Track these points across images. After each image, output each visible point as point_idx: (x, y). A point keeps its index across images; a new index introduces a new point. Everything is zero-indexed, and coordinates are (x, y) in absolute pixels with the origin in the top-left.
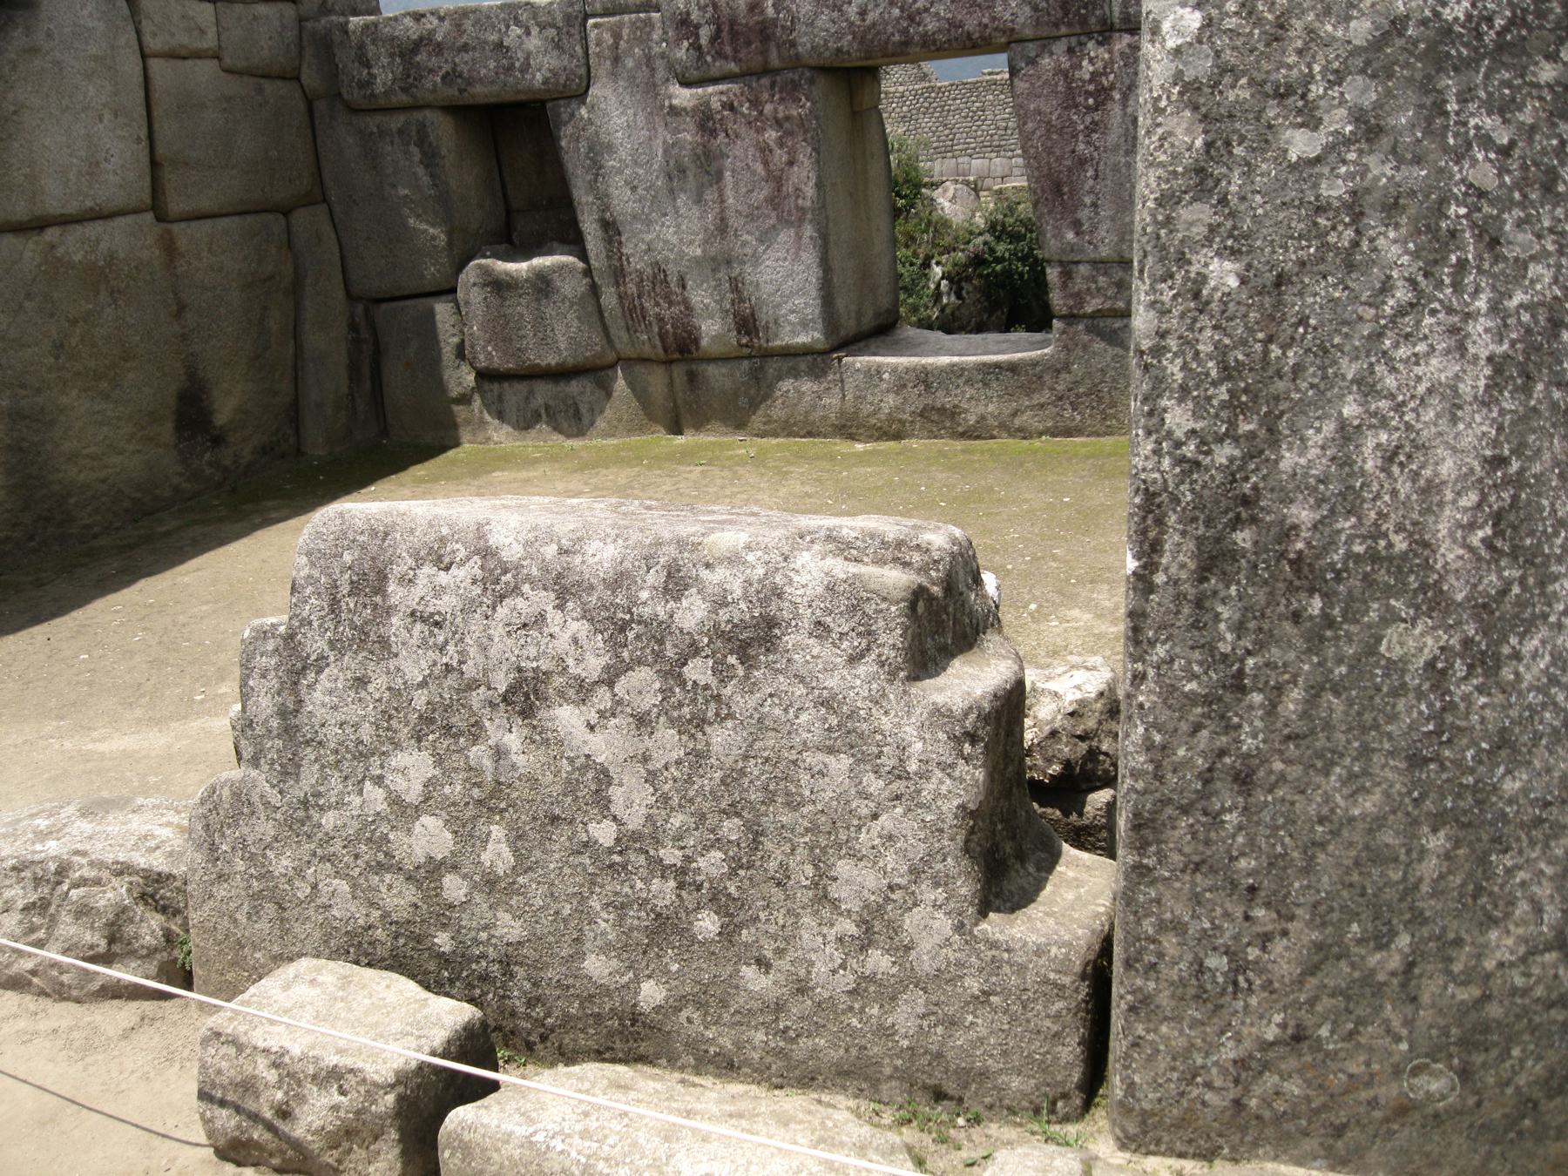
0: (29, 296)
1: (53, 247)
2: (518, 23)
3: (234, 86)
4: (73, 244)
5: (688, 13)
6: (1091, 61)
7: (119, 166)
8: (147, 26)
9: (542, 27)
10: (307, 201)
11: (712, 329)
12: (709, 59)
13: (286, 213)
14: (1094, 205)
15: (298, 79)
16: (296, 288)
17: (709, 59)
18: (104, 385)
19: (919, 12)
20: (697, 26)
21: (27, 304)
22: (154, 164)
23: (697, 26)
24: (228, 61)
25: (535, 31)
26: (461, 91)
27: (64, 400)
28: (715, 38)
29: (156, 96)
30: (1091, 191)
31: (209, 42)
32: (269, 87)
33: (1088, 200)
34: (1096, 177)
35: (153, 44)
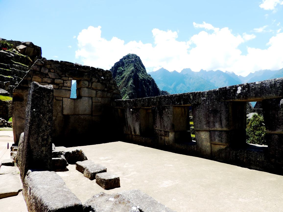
35: (93, 101)
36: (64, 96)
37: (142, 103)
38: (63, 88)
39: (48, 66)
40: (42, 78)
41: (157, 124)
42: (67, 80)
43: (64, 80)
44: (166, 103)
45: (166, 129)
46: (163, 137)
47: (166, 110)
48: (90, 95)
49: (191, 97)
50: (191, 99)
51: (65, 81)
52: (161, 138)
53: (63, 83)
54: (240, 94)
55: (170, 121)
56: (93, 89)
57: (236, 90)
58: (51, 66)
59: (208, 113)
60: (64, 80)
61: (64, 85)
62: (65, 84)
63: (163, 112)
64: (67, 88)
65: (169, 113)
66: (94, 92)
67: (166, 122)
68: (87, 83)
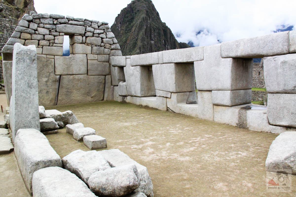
0: (71, 81)
1: (74, 77)
3: (99, 63)
4: (76, 77)
7: (83, 69)
8: (88, 57)
10: (108, 75)
13: (105, 76)
15: (109, 62)
16: (105, 83)
18: (78, 90)
21: (70, 82)
22: (87, 70)
24: (98, 61)
27: (73, 91)
29: (88, 64)
31: (96, 58)
32: (104, 63)
35: (88, 59)
36: (56, 54)
38: (54, 45)
39: (38, 21)
40: (31, 35)
42: (58, 36)
43: (55, 36)
48: (85, 52)
51: (56, 37)
53: (54, 39)
56: (88, 45)
58: (40, 20)
60: (55, 36)
61: (56, 42)
62: (56, 41)
64: (59, 45)
66: (89, 48)
68: (80, 37)
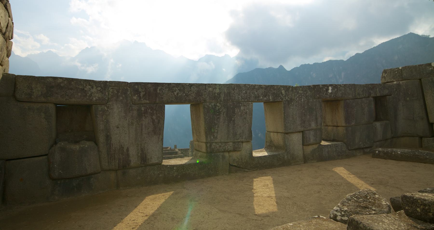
2: (90, 85)
5: (138, 89)
6: (218, 107)
9: (97, 87)
11: (134, 160)
12: (142, 99)
14: (217, 132)
17: (142, 99)
19: (189, 95)
20: (140, 92)
23: (140, 92)
25: (95, 87)
26: (66, 100)
28: (144, 95)
30: (217, 129)
33: (216, 131)
34: (218, 127)
37: (178, 94)
41: (217, 132)
44: (242, 97)
45: (238, 139)
46: (227, 154)
47: (242, 108)
49: (283, 92)
50: (282, 95)
52: (224, 157)
54: (331, 93)
55: (247, 125)
57: (328, 90)
59: (303, 111)
63: (236, 111)
65: (246, 113)
67: (240, 127)
